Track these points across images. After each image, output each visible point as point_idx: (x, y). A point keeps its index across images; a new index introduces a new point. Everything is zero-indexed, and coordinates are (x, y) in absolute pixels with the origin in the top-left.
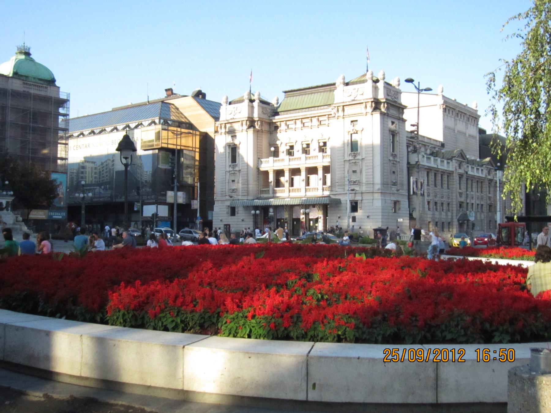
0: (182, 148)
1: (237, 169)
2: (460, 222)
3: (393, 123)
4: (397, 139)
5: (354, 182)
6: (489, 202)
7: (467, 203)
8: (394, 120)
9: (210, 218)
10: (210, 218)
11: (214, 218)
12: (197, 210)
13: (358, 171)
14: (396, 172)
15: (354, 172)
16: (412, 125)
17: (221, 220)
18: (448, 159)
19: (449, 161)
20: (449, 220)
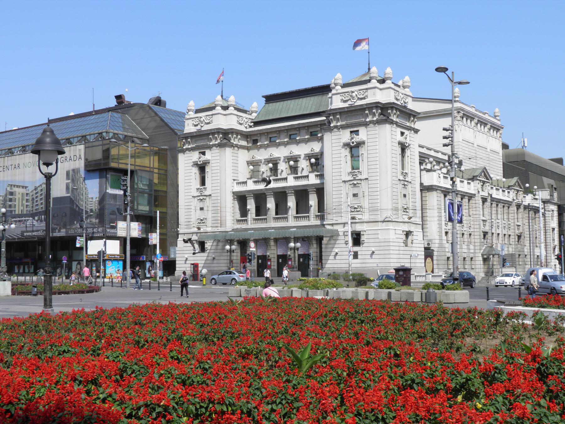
0: (137, 168)
2: (485, 257)
3: (402, 134)
4: (408, 153)
6: (517, 232)
7: (493, 234)
8: (403, 131)
9: (172, 256)
10: (172, 256)
11: (177, 255)
12: (155, 246)
13: (360, 195)
14: (407, 196)
15: (355, 195)
16: (444, 129)
18: (469, 179)
19: (469, 181)
20: (472, 255)
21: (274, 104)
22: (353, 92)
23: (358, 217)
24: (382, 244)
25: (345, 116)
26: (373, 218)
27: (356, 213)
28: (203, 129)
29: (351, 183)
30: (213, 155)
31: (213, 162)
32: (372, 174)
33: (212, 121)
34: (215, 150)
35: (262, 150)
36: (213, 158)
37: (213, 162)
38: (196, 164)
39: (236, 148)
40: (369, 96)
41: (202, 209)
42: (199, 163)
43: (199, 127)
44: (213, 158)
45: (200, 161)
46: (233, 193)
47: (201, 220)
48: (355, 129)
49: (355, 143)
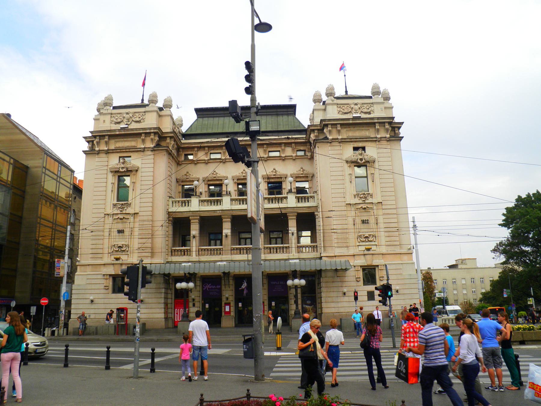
1: (130, 210)
5: (366, 237)
11: (74, 296)
12: (62, 278)
13: (372, 220)
17: (92, 301)
21: (211, 119)
22: (356, 104)
23: (374, 248)
24: (407, 281)
25: (345, 130)
26: (390, 250)
27: (367, 243)
28: (130, 127)
29: (360, 206)
30: (144, 161)
31: (143, 170)
32: (387, 198)
33: (143, 119)
34: (149, 157)
35: (201, 166)
36: (143, 166)
37: (143, 170)
38: (115, 172)
39: (171, 158)
40: (375, 111)
41: (120, 232)
42: (121, 170)
43: (123, 125)
44: (143, 166)
45: (123, 168)
46: (169, 213)
47: (119, 247)
48: (360, 145)
49: (364, 161)
